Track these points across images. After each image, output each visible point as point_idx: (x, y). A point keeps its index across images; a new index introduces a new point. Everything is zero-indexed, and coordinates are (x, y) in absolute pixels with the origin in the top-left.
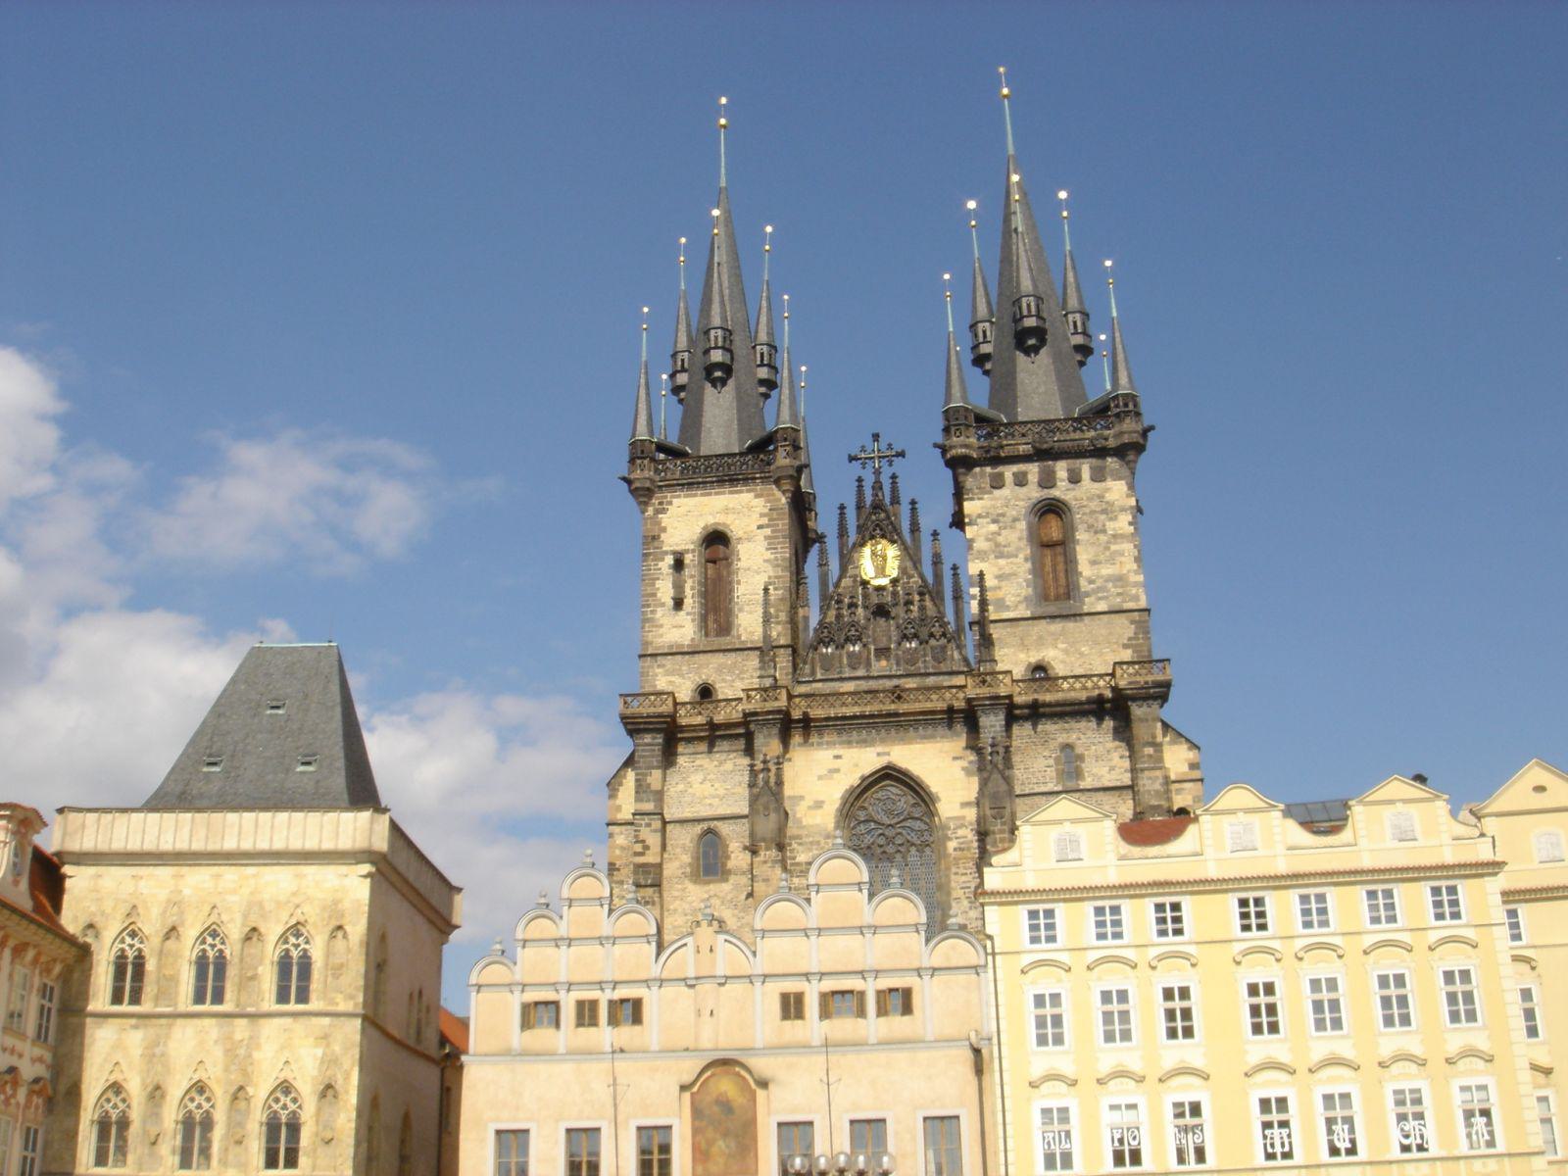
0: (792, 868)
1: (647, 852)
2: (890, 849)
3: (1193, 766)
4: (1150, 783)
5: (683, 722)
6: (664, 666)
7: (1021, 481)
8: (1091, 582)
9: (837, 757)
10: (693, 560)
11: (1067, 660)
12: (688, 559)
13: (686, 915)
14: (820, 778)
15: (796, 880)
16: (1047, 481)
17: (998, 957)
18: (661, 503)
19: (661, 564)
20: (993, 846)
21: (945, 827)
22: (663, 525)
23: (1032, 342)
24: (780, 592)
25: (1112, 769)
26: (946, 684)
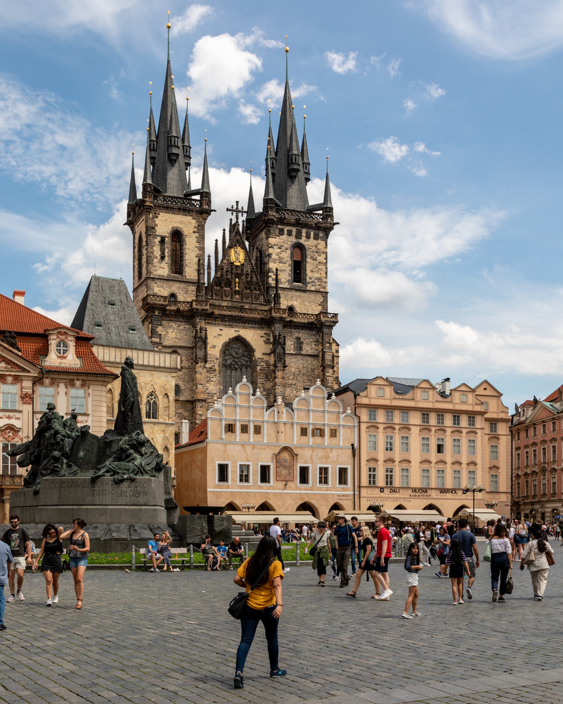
2: (237, 366)
4: (328, 357)
5: (168, 308)
6: (157, 283)
7: (290, 233)
8: (310, 279)
9: (221, 330)
11: (300, 306)
12: (167, 239)
14: (215, 337)
16: (299, 236)
19: (155, 240)
20: (278, 371)
21: (256, 361)
23: (294, 174)
25: (312, 348)
26: (259, 308)
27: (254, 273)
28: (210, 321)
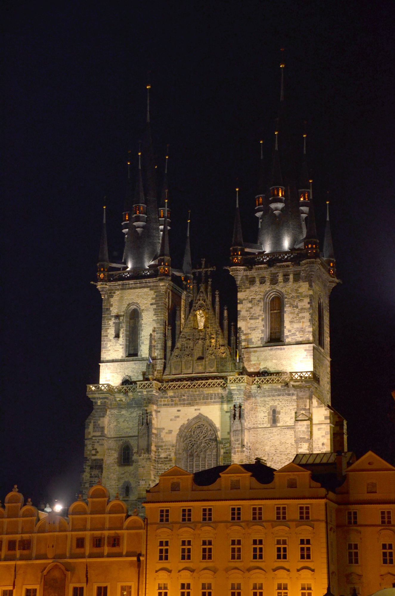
0: (158, 460)
1: (97, 454)
3: (326, 418)
7: (262, 282)
8: (289, 331)
9: (179, 411)
10: (123, 320)
13: (115, 480)
14: (171, 420)
15: (160, 465)
17: (148, 527)
18: (110, 293)
20: (235, 454)
21: (221, 443)
22: (111, 303)
24: (159, 335)
27: (220, 336)
28: (166, 403)
